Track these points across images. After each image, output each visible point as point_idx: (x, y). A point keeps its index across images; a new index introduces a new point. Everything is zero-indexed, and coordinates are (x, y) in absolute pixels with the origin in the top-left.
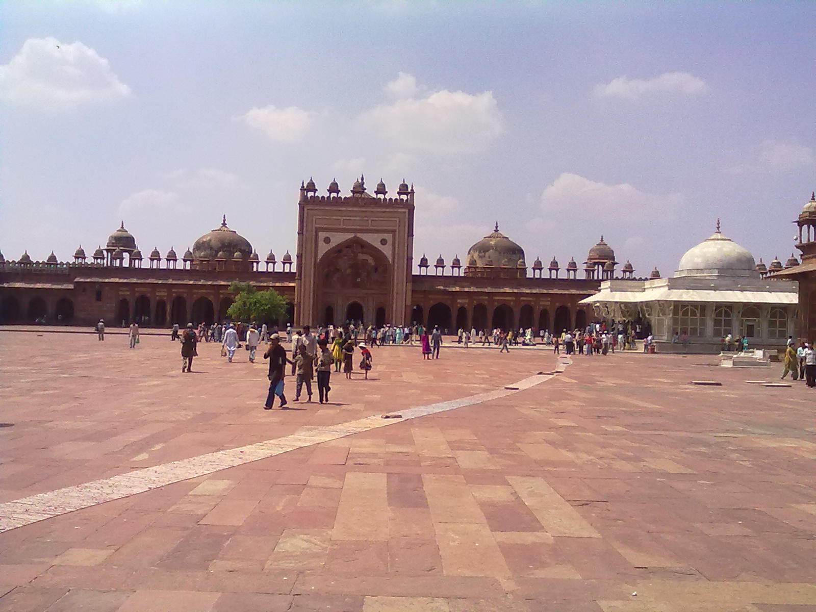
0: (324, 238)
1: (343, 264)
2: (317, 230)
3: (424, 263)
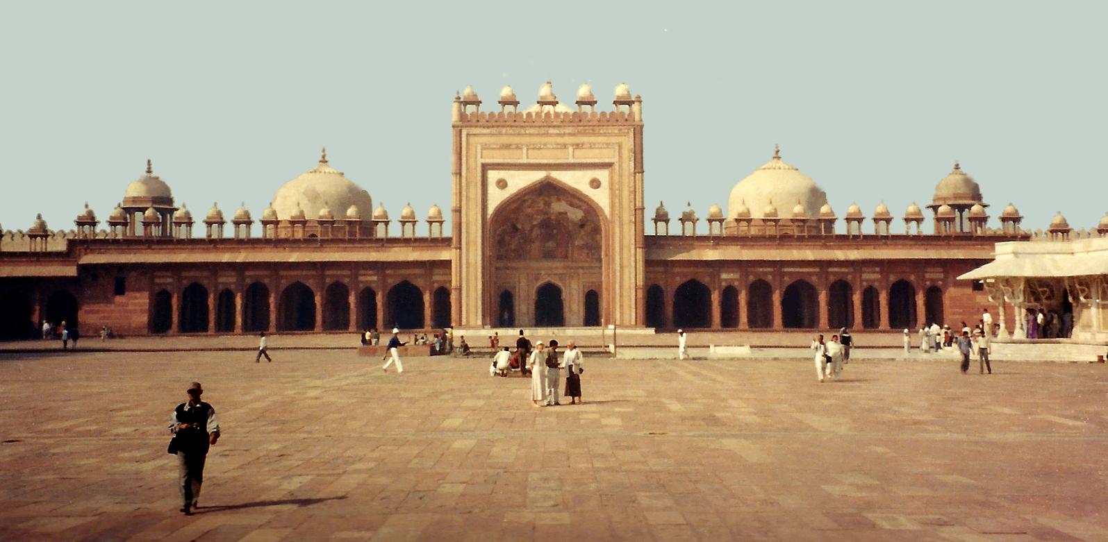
0: (496, 180)
3: (661, 217)
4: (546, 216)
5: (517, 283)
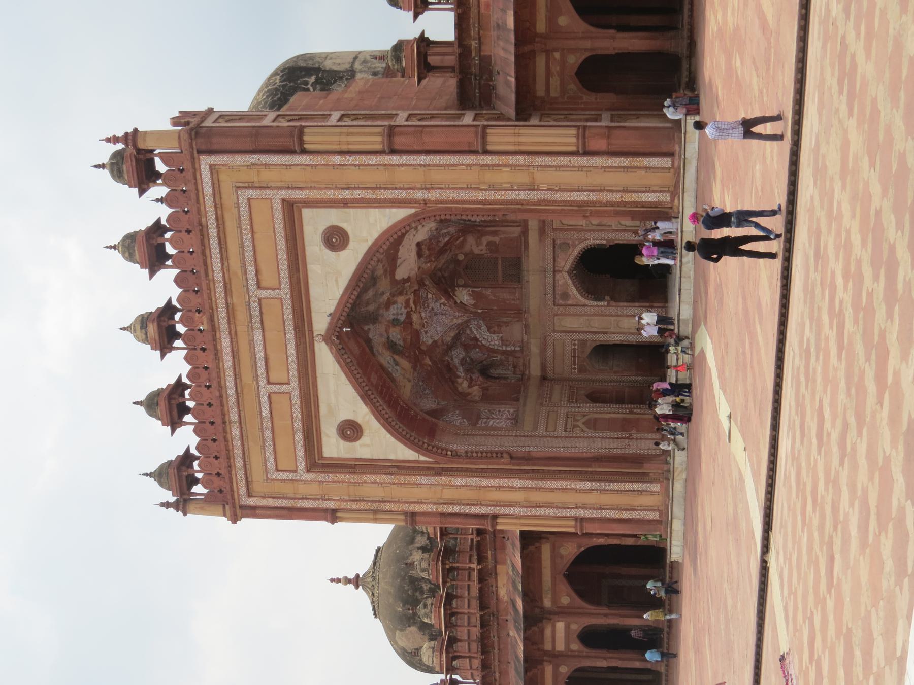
1: (439, 322)
2: (316, 462)
4: (427, 283)
5: (576, 336)
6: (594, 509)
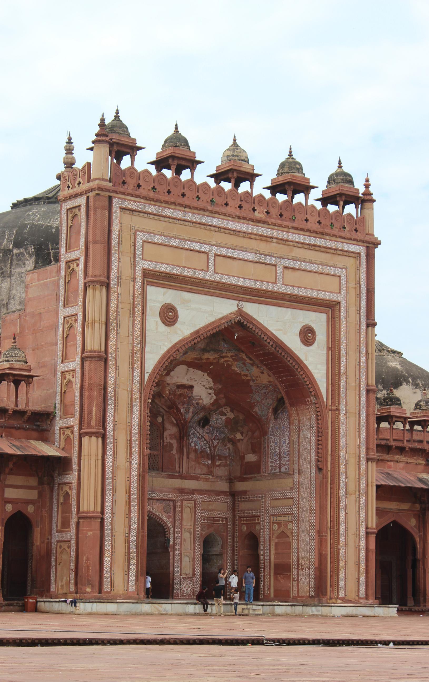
0: (160, 305)
6: (112, 529)
